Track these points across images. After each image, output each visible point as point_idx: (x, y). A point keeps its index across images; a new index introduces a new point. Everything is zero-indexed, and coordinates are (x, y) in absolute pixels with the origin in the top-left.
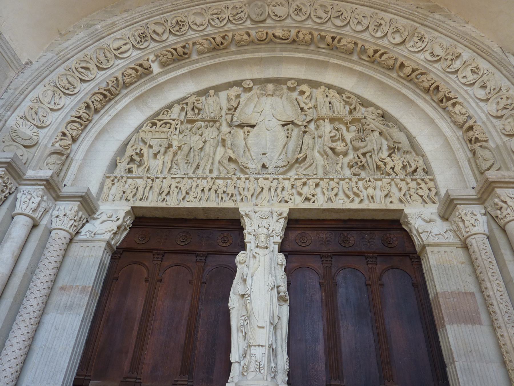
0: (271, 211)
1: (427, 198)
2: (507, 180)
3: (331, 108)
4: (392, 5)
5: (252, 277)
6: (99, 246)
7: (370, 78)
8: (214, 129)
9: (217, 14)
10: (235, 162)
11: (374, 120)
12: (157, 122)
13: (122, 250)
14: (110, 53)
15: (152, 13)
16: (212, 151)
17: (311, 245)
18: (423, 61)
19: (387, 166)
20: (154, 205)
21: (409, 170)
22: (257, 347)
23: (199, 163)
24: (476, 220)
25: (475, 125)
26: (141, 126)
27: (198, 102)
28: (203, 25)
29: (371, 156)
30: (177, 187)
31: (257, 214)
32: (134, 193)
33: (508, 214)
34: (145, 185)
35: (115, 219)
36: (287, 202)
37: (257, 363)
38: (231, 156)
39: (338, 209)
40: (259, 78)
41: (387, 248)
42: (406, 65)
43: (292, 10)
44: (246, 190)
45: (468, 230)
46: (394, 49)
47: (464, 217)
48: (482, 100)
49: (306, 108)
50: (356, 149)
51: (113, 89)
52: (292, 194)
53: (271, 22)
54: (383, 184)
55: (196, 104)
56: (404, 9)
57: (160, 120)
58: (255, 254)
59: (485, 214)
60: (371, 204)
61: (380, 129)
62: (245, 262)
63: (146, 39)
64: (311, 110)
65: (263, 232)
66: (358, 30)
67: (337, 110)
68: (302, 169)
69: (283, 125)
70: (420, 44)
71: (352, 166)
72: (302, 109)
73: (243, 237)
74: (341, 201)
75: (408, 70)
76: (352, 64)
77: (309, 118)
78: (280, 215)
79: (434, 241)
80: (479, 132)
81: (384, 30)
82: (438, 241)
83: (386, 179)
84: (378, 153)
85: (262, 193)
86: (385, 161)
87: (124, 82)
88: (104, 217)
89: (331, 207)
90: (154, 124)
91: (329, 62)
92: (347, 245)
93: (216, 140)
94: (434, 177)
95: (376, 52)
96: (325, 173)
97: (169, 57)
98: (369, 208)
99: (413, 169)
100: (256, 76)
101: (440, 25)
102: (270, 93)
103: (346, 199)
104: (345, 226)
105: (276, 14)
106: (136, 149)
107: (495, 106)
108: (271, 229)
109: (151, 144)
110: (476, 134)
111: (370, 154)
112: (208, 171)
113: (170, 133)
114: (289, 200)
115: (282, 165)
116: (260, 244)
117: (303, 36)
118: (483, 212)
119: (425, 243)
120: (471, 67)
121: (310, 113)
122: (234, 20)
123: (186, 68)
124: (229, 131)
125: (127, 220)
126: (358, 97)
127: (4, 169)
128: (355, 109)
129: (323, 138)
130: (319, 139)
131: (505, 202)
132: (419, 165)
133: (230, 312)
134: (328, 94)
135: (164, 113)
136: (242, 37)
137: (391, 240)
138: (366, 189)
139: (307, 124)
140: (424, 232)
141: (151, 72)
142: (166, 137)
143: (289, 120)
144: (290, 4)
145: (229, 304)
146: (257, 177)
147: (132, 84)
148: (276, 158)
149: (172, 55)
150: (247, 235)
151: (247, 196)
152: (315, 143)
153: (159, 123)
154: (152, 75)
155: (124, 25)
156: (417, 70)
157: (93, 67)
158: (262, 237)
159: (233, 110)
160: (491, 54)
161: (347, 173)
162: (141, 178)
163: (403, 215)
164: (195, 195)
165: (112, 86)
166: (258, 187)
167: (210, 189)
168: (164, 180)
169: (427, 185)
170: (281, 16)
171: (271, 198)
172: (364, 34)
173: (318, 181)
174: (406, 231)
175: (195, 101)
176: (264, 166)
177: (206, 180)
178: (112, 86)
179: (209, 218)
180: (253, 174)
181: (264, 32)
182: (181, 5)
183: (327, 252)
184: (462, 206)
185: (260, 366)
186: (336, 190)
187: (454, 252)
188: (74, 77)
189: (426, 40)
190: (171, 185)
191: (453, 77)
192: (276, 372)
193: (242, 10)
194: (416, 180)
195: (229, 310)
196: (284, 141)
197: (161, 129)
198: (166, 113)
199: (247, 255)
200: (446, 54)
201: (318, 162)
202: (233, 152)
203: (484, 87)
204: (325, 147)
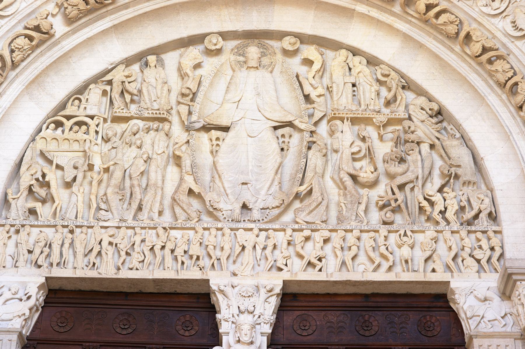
0: (256, 284)
1: (486, 263)
3: (356, 93)
6: (8, 338)
7: (421, 46)
8: (162, 134)
10: (199, 196)
11: (423, 121)
12: (64, 120)
13: (36, 342)
16: (160, 178)
17: (315, 333)
18: (500, 30)
20: (79, 274)
21: (469, 215)
23: (141, 199)
27: (130, 80)
29: (412, 189)
30: (110, 243)
31: (237, 289)
32: (46, 253)
34: (62, 239)
35: (24, 298)
36: (280, 269)
38: (193, 188)
39: (356, 282)
40: (235, 30)
41: (423, 337)
42: (474, 38)
44: (218, 248)
50: (391, 177)
52: (287, 257)
55: (127, 83)
60: (404, 273)
61: (431, 140)
64: (322, 98)
67: (365, 100)
68: (305, 213)
69: (275, 128)
71: (384, 206)
72: (307, 97)
73: (215, 326)
74: (361, 268)
75: (477, 48)
76: (392, 18)
77: (318, 115)
78: (270, 291)
79: (485, 330)
82: (491, 330)
84: (423, 186)
85: (242, 253)
86: (433, 199)
87: (12, 61)
88: (7, 295)
89: (345, 279)
90: (59, 124)
91: (354, 10)
92: (367, 333)
93: (165, 156)
95: (429, 7)
96: (340, 219)
97: (81, 8)
98: (401, 280)
99: (473, 213)
102: (254, 63)
103: (368, 263)
104: (365, 304)
106: (36, 172)
108: (257, 313)
109: (59, 163)
111: (411, 185)
112: (157, 214)
113: (88, 141)
115: (274, 206)
116: (242, 338)
119: (472, 334)
121: (320, 106)
123: (107, 19)
124: (186, 140)
125: (40, 297)
126: (402, 76)
128: (395, 97)
129: (339, 154)
130: (334, 154)
132: (483, 207)
134: (351, 67)
135: (73, 101)
137: (432, 325)
138: (400, 247)
139: (313, 128)
140: (473, 316)
141: (53, 36)
142: (82, 149)
146: (234, 227)
147: (22, 61)
148: (263, 192)
150: (222, 322)
151: (219, 259)
152: (327, 161)
153: (68, 124)
154: (53, 40)
156: (491, 49)
158: (246, 328)
159: (191, 96)
161: (375, 216)
162: (55, 226)
163: (450, 289)
164: (140, 257)
166: (237, 244)
167: (163, 247)
168: (90, 230)
171: (256, 262)
173: (327, 234)
174: (454, 311)
175: (124, 79)
176: (244, 206)
177: (154, 231)
179: (162, 292)
180: (228, 220)
183: (338, 345)
186: (354, 249)
187: (510, 346)
190: (101, 240)
194: (475, 232)
196: (276, 161)
197: (71, 135)
198: (77, 102)
201: (331, 197)
202: (195, 180)
204: (342, 172)
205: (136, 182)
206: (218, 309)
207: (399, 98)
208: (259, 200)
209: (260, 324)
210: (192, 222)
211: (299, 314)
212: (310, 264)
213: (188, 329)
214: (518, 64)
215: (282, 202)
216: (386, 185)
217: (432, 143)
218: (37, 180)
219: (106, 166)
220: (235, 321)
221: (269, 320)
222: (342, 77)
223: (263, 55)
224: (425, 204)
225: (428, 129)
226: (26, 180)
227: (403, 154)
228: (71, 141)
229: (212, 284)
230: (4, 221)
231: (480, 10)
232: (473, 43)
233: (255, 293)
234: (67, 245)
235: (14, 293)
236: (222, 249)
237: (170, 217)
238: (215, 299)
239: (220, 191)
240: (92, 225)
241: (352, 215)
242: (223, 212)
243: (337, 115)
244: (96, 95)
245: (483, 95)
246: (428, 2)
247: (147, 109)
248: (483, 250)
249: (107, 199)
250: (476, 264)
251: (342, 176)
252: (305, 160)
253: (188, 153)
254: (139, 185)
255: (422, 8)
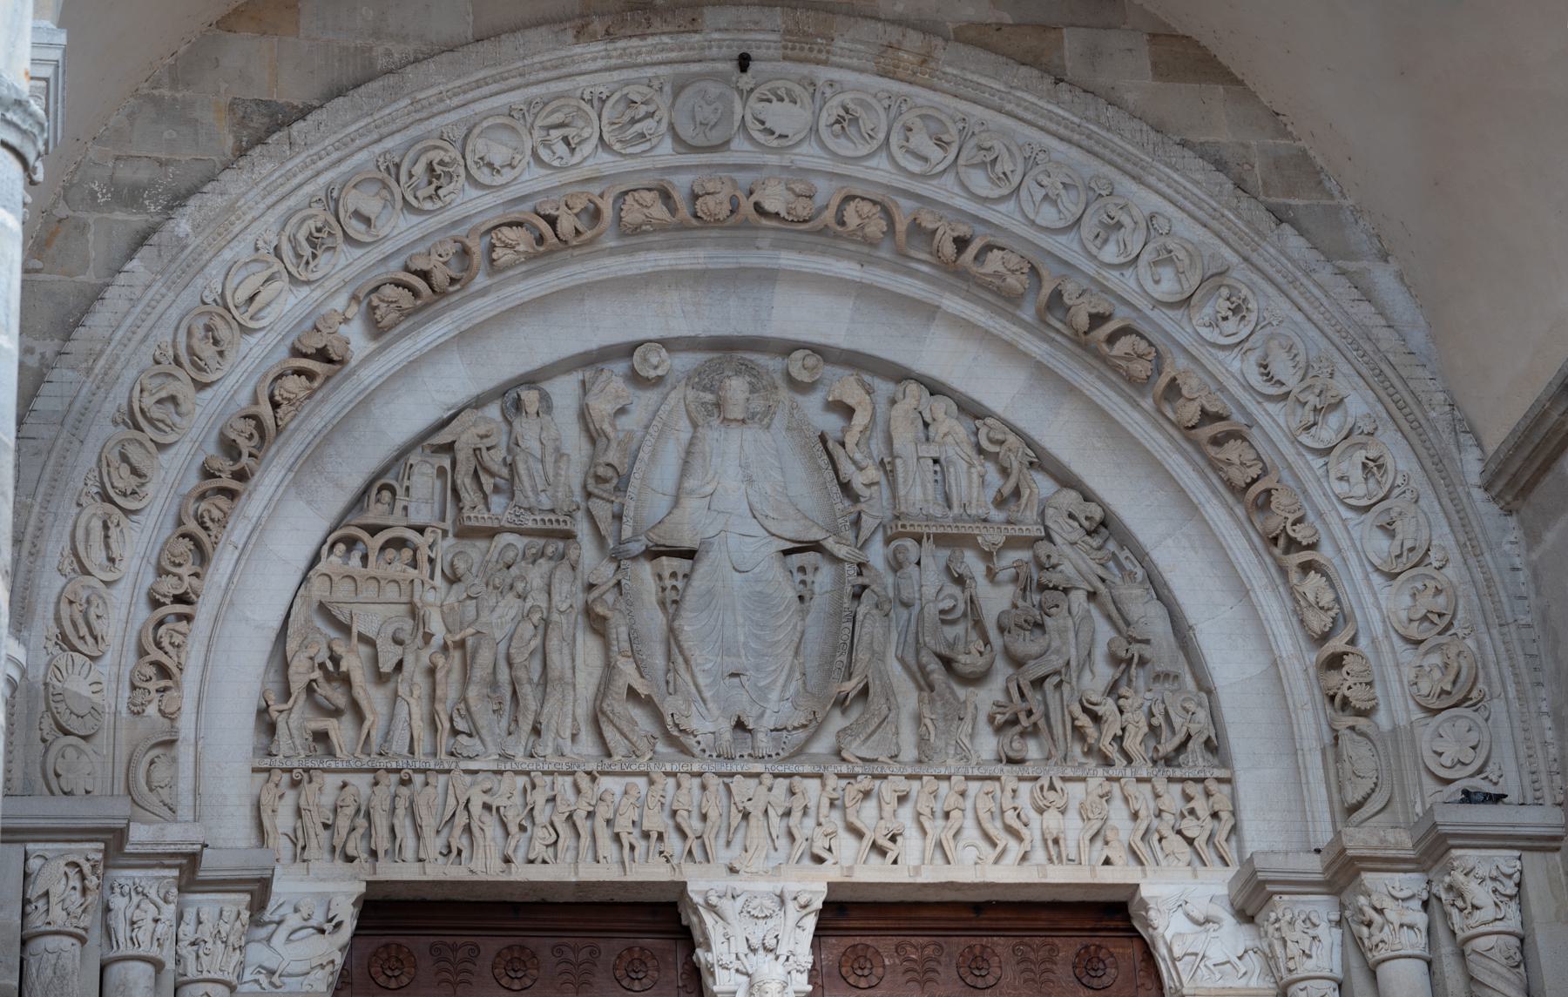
1: (1204, 846)
2: (1391, 853)
4: (1162, 167)
7: (1070, 389)
9: (562, 125)
11: (1073, 544)
12: (364, 535)
14: (228, 323)
15: (346, 145)
16: (568, 664)
18: (1233, 376)
19: (1105, 727)
21: (1168, 746)
24: (1314, 938)
25: (1347, 654)
26: (316, 559)
28: (513, 168)
29: (1059, 686)
31: (740, 901)
33: (1382, 941)
35: (328, 927)
36: (819, 860)
42: (1185, 391)
43: (825, 119)
45: (1291, 965)
46: (1155, 315)
47: (1287, 933)
48: (1377, 570)
49: (858, 481)
50: (1017, 662)
51: (252, 462)
53: (747, 146)
54: (1090, 798)
55: (484, 452)
56: (1195, 190)
57: (374, 530)
59: (1339, 923)
61: (1090, 583)
63: (329, 242)
64: (875, 488)
66: (1044, 223)
67: (959, 494)
70: (1233, 320)
72: (846, 488)
74: (971, 854)
75: (1191, 413)
76: (1015, 329)
78: (804, 907)
79: (1209, 984)
80: (1355, 680)
81: (1129, 248)
82: (1220, 983)
83: (1096, 783)
86: (1100, 710)
87: (277, 426)
88: (294, 921)
90: (351, 542)
91: (938, 307)
94: (1233, 773)
99: (1176, 741)
100: (681, 327)
101: (1296, 279)
103: (984, 846)
104: (974, 924)
105: (768, 125)
107: (1407, 600)
108: (783, 950)
109: (362, 630)
110: (1347, 684)
111: (1056, 679)
113: (417, 582)
114: (825, 854)
117: (858, 221)
118: (1335, 916)
119: (1185, 991)
120: (1363, 453)
122: (620, 141)
126: (1029, 443)
127: (102, 846)
131: (1380, 911)
132: (1194, 728)
134: (928, 419)
135: (379, 491)
136: (645, 210)
138: (1041, 811)
143: (806, 539)
144: (818, 95)
149: (415, 293)
150: (718, 970)
155: (262, 206)
156: (1220, 418)
157: (183, 389)
160: (1421, 426)
163: (1137, 899)
165: (251, 455)
166: (733, 808)
167: (591, 815)
168: (442, 778)
169: (1211, 799)
170: (784, 133)
172: (1062, 239)
173: (903, 785)
176: (740, 725)
177: (569, 779)
178: (251, 455)
181: (723, 196)
182: (442, 100)
184: (1285, 897)
188: (141, 444)
189: (1253, 317)
190: (468, 801)
191: (1317, 463)
193: (651, 108)
194: (1182, 780)
198: (386, 495)
200: (1304, 385)
202: (638, 668)
203: (1388, 529)
204: (923, 652)
205: (522, 674)
207: (1026, 493)
208: (768, 712)
210: (641, 760)
212: (875, 847)
214: (1268, 449)
215: (812, 717)
216: (1008, 680)
217: (1091, 589)
218: (322, 666)
219: (458, 638)
222: (913, 445)
223: (753, 389)
224: (1084, 721)
225: (1083, 559)
226: (302, 670)
227: (1037, 612)
228: (382, 582)
230: (267, 761)
231: (1198, 334)
232: (1181, 401)
234: (401, 812)
235: (306, 916)
236: (704, 817)
237: (590, 744)
238: (694, 919)
239: (689, 693)
240: (446, 767)
241: (947, 744)
242: (699, 738)
243: (909, 529)
244: (425, 478)
245: (1196, 501)
246: (1094, 311)
247: (530, 510)
248: (1198, 819)
249: (468, 710)
250: (1188, 849)
251: (924, 660)
252: (850, 625)
253: (620, 611)
254: (530, 681)
255: (1082, 321)
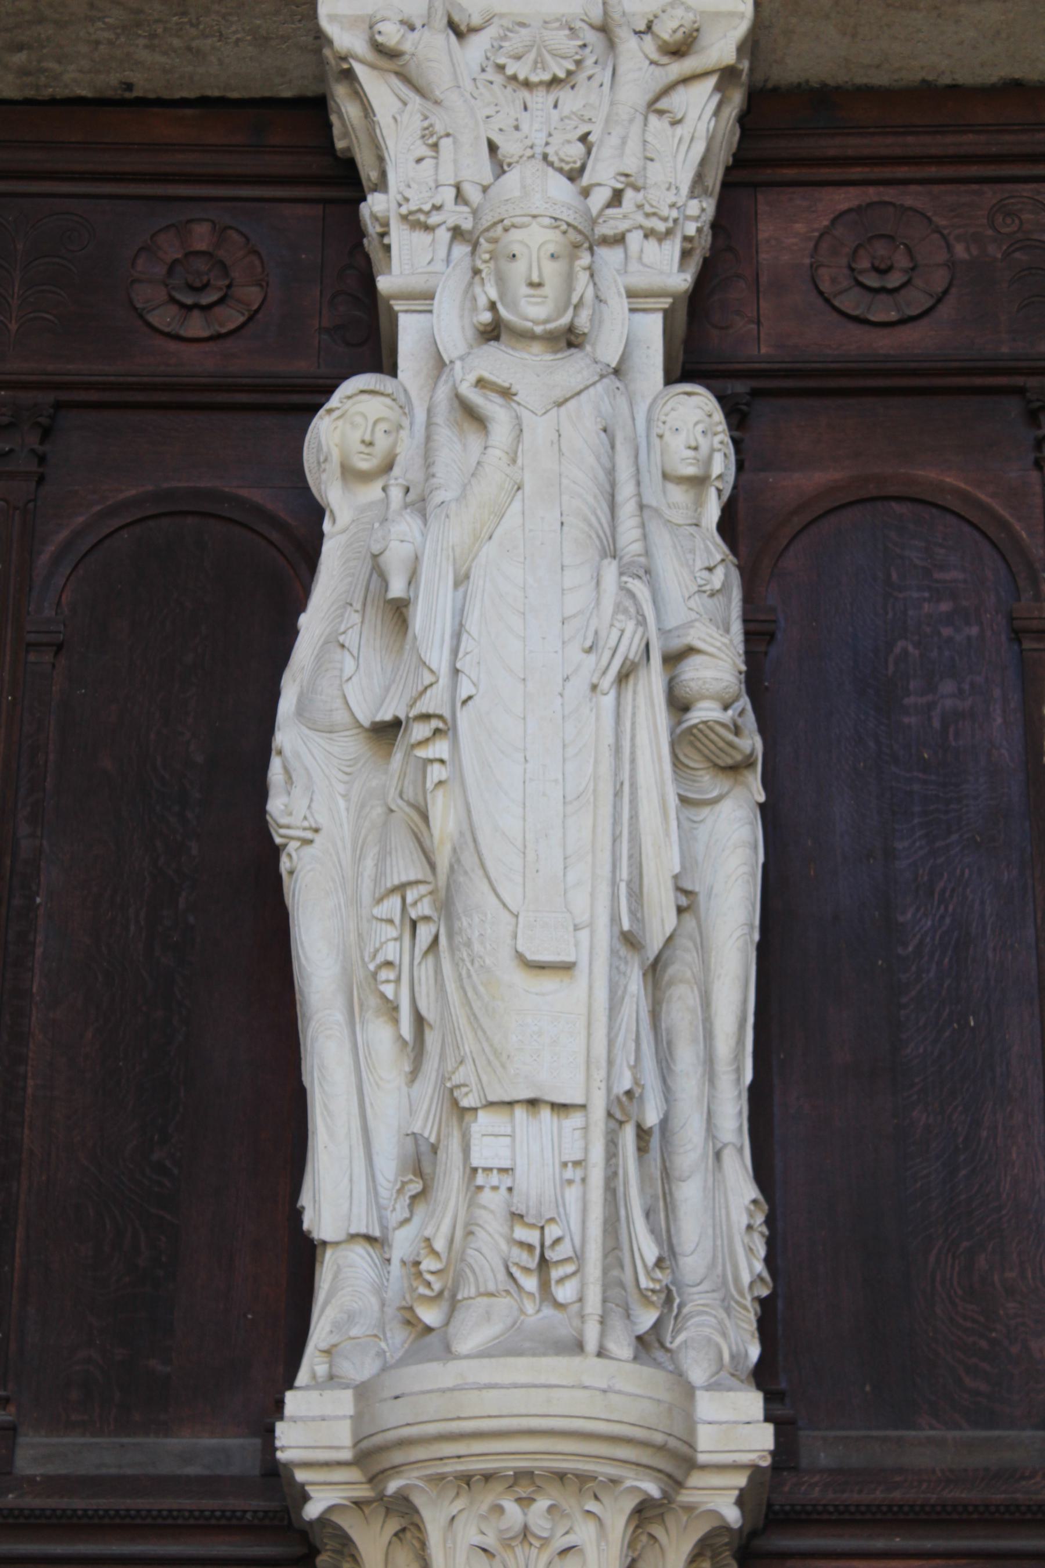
5: (461, 580)
17: (944, 311)
22: (520, 1112)
31: (478, 45)
37: (521, 1233)
58: (475, 397)
62: (388, 467)
65: (537, 204)
78: (678, 51)
116: (513, 307)
133: (285, 864)
145: (275, 805)
150: (399, 237)
179: (47, 93)
185: (551, 1255)
192: (669, 1300)
195: (274, 852)
199: (406, 408)
206: (374, 175)
209: (620, 240)
211: (844, 206)
213: (206, 300)
220: (467, 225)
221: (674, 214)
229: (332, 18)
233: (589, 62)
238: (351, 110)
